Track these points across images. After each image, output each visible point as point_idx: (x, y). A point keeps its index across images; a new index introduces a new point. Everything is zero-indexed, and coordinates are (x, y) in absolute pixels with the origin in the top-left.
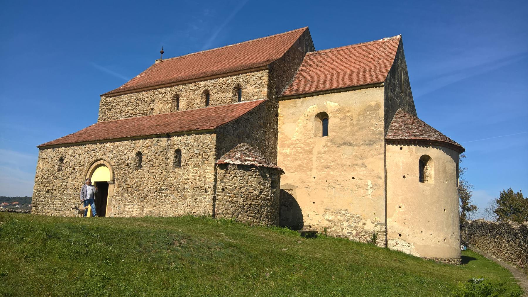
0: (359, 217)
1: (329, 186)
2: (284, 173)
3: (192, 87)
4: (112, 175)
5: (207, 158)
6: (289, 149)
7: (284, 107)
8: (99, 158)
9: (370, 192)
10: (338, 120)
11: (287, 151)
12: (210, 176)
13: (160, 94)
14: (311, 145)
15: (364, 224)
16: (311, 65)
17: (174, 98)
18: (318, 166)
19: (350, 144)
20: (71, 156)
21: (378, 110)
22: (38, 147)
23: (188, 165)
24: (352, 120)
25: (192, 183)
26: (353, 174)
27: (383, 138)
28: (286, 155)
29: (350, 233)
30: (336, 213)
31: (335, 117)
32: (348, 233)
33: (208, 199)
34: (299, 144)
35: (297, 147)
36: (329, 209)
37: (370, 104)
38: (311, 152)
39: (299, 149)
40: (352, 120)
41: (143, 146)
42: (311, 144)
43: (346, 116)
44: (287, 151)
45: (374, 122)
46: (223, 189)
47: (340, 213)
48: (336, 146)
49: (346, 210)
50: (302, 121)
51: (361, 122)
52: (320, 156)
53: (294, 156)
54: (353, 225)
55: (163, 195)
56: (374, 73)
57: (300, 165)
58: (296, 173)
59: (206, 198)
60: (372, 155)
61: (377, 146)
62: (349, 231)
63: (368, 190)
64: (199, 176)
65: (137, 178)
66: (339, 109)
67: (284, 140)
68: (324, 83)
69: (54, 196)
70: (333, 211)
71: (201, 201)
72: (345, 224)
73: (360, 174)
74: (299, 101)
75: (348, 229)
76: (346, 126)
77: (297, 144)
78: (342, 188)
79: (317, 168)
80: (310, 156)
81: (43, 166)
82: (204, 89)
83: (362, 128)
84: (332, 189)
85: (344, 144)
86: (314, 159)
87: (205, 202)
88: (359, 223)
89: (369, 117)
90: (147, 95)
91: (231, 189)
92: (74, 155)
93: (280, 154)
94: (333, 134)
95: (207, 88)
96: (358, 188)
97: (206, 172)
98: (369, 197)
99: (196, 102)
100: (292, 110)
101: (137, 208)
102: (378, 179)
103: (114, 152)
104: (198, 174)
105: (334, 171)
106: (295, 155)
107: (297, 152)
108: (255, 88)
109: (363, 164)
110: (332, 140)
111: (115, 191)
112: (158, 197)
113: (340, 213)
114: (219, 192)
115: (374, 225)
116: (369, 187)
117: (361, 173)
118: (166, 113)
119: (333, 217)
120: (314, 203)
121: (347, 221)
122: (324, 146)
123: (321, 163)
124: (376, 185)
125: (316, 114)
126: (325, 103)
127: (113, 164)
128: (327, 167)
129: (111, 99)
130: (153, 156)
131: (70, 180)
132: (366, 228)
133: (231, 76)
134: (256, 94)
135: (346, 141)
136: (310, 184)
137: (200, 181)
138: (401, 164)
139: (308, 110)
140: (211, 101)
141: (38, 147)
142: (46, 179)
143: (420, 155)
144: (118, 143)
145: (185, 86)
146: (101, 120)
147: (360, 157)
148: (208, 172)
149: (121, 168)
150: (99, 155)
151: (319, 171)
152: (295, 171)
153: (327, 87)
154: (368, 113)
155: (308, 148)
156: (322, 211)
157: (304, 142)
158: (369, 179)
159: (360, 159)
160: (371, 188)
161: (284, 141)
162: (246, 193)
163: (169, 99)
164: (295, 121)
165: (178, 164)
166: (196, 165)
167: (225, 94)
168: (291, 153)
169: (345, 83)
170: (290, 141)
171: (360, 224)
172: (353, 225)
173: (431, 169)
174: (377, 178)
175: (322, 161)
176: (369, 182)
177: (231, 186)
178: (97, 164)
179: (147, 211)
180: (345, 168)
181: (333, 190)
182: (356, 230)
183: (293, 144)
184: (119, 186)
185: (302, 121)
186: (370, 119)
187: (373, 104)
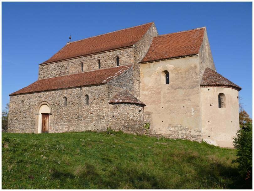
2: (146, 105)
3: (90, 58)
4: (51, 110)
6: (147, 92)
7: (144, 68)
8: (43, 100)
9: (193, 114)
10: (175, 75)
11: (146, 93)
12: (105, 109)
13: (72, 62)
15: (190, 132)
16: (157, 43)
19: (181, 88)
21: (196, 69)
22: (9, 95)
26: (184, 105)
28: (145, 95)
29: (183, 137)
31: (172, 73)
32: (181, 137)
33: (105, 122)
36: (171, 125)
38: (160, 93)
40: (182, 75)
42: (160, 88)
43: (178, 73)
44: (146, 93)
45: (194, 75)
46: (113, 116)
48: (174, 89)
49: (180, 125)
50: (154, 76)
51: (187, 76)
53: (150, 96)
54: (184, 132)
55: (80, 120)
56: (192, 48)
57: (154, 101)
58: (152, 105)
59: (103, 121)
60: (193, 94)
61: (196, 89)
62: (182, 136)
63: (192, 113)
64: (99, 109)
66: (174, 68)
67: (144, 87)
68: (165, 54)
69: (20, 122)
71: (101, 123)
72: (180, 132)
73: (187, 105)
74: (152, 64)
75: (181, 135)
76: (179, 78)
77: (152, 89)
79: (163, 102)
80: (159, 96)
81: (13, 105)
83: (188, 79)
84: (172, 113)
85: (178, 88)
86: (162, 97)
89: (191, 73)
90: (65, 64)
92: (29, 99)
93: (142, 94)
94: (172, 82)
95: (99, 58)
98: (192, 117)
99: (93, 66)
100: (149, 70)
101: (66, 128)
102: (197, 107)
103: (51, 97)
104: (99, 108)
105: (173, 104)
106: (150, 95)
107: (152, 93)
108: (126, 58)
109: (189, 99)
110: (171, 86)
111: (53, 118)
114: (111, 118)
115: (195, 132)
116: (192, 112)
117: (188, 104)
118: (76, 73)
119: (173, 128)
121: (181, 131)
122: (167, 90)
123: (166, 99)
124: (196, 110)
125: (162, 71)
126: (166, 66)
128: (169, 101)
129: (45, 66)
130: (73, 99)
131: (28, 112)
132: (191, 134)
133: (112, 51)
135: (179, 86)
136: (160, 112)
137: (100, 112)
138: (209, 98)
139: (157, 69)
140: (101, 66)
141: (9, 95)
142: (15, 113)
143: (219, 93)
144: (53, 92)
148: (104, 107)
149: (55, 106)
150: (43, 99)
151: (165, 104)
152: (152, 104)
153: (167, 56)
154: (191, 71)
155: (158, 91)
156: (167, 125)
157: (156, 88)
158: (192, 107)
159: (187, 96)
160: (193, 112)
161: (144, 87)
162: (126, 118)
164: (150, 76)
165: (87, 103)
168: (148, 94)
169: (177, 54)
170: (148, 87)
171: (188, 132)
172: (184, 132)
173: (226, 100)
174: (197, 106)
175: (166, 98)
176: (193, 109)
177: (117, 114)
178: (42, 103)
179: (71, 129)
180: (179, 102)
181: (173, 113)
182: (186, 135)
183: (149, 89)
184: (55, 116)
185: (154, 76)
186: (192, 74)
187: (193, 66)
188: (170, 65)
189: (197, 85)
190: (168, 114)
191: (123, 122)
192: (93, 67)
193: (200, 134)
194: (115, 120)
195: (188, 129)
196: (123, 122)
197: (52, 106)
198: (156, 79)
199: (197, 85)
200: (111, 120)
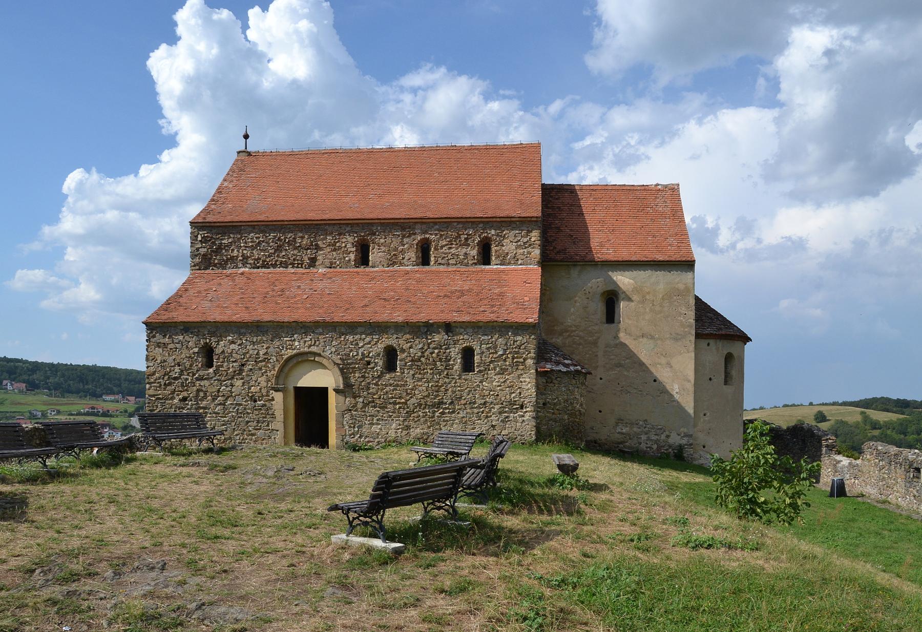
0: (661, 429)
1: (621, 390)
5: (522, 363)
6: (561, 338)
8: (306, 349)
12: (527, 387)
14: (596, 335)
15: (668, 436)
17: (358, 245)
18: (606, 364)
19: (652, 338)
20: (233, 342)
23: (489, 370)
24: (653, 305)
25: (498, 395)
27: (693, 332)
30: (632, 424)
34: (577, 332)
35: (574, 335)
36: (622, 420)
37: (676, 286)
38: (595, 343)
39: (578, 338)
41: (397, 338)
46: (544, 404)
47: (637, 424)
48: (632, 338)
51: (666, 309)
52: (610, 350)
59: (523, 416)
65: (391, 385)
66: (635, 288)
70: (627, 421)
77: (575, 331)
78: (640, 393)
79: (604, 367)
82: (419, 238)
84: (626, 394)
86: (600, 354)
87: (523, 420)
88: (662, 435)
91: (555, 404)
92: (239, 342)
96: (661, 393)
97: (521, 382)
105: (628, 371)
108: (517, 247)
109: (669, 365)
112: (437, 414)
113: (637, 424)
114: (539, 407)
115: (680, 437)
120: (600, 411)
121: (646, 434)
123: (611, 359)
125: (602, 291)
127: (339, 362)
128: (619, 365)
129: (214, 231)
130: (420, 354)
134: (522, 257)
138: (708, 364)
143: (725, 352)
145: (382, 228)
146: (197, 267)
147: (664, 354)
148: (525, 382)
155: (590, 339)
159: (664, 356)
161: (554, 326)
162: (570, 408)
163: (349, 245)
166: (503, 371)
167: (464, 250)
175: (612, 357)
183: (567, 331)
187: (681, 286)
188: (623, 280)
189: (690, 333)
190: (615, 394)
191: (566, 417)
192: (407, 258)
193: (691, 441)
194: (548, 412)
195: (663, 430)
196: (566, 417)
197: (345, 370)
198: (587, 307)
199: (690, 333)
200: (540, 414)
